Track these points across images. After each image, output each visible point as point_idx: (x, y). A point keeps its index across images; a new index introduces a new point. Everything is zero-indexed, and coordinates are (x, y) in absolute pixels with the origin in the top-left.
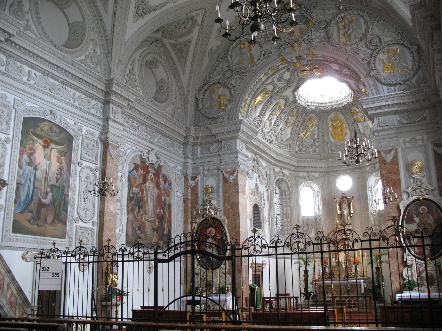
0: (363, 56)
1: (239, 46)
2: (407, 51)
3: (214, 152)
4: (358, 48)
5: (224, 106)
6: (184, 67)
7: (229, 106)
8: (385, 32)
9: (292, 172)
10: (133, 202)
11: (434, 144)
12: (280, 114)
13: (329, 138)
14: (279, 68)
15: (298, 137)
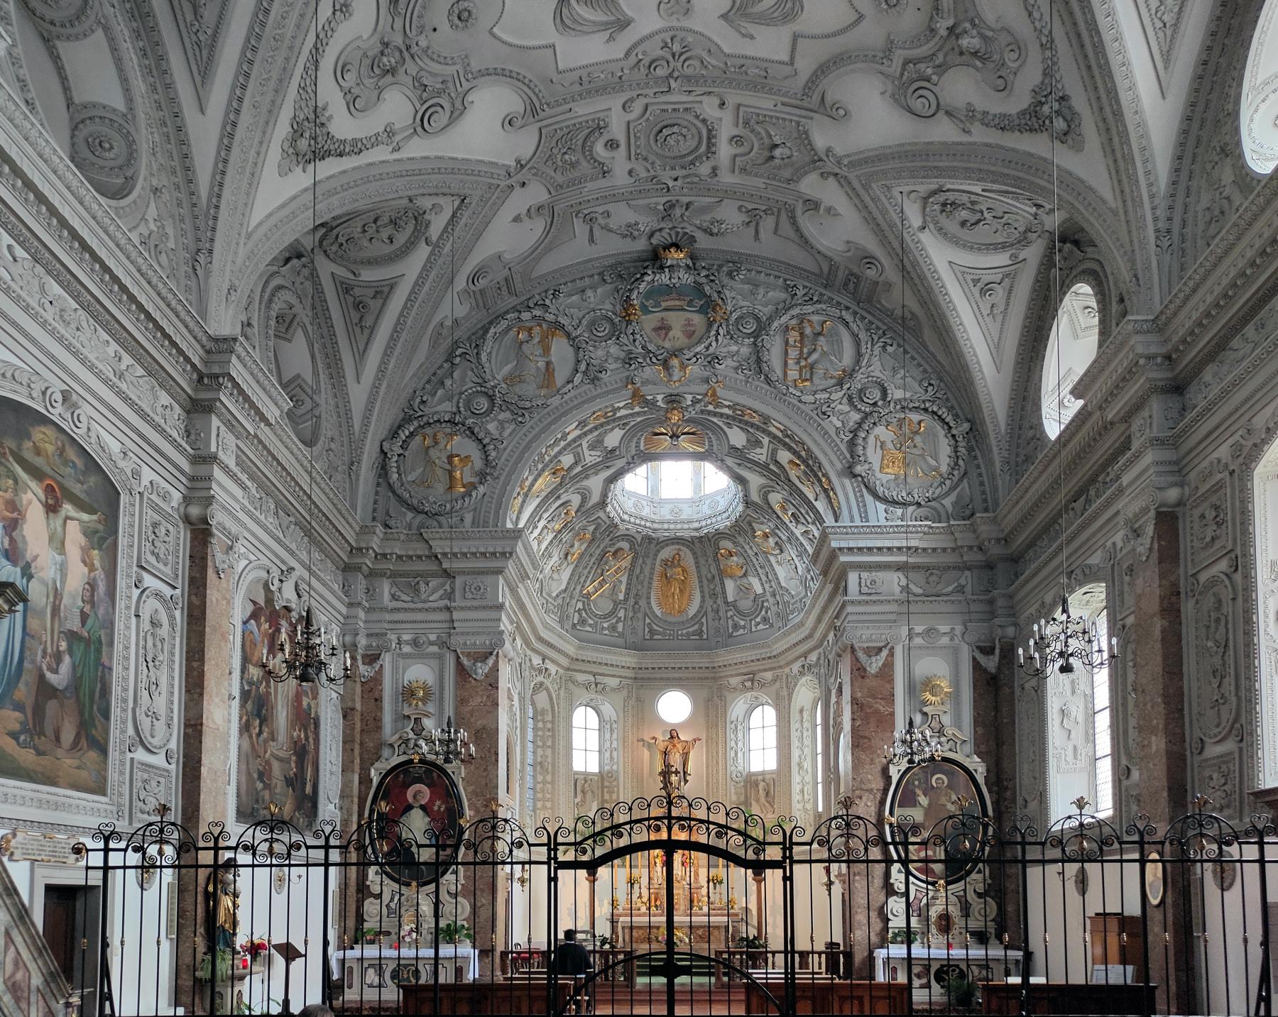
13: (649, 603)
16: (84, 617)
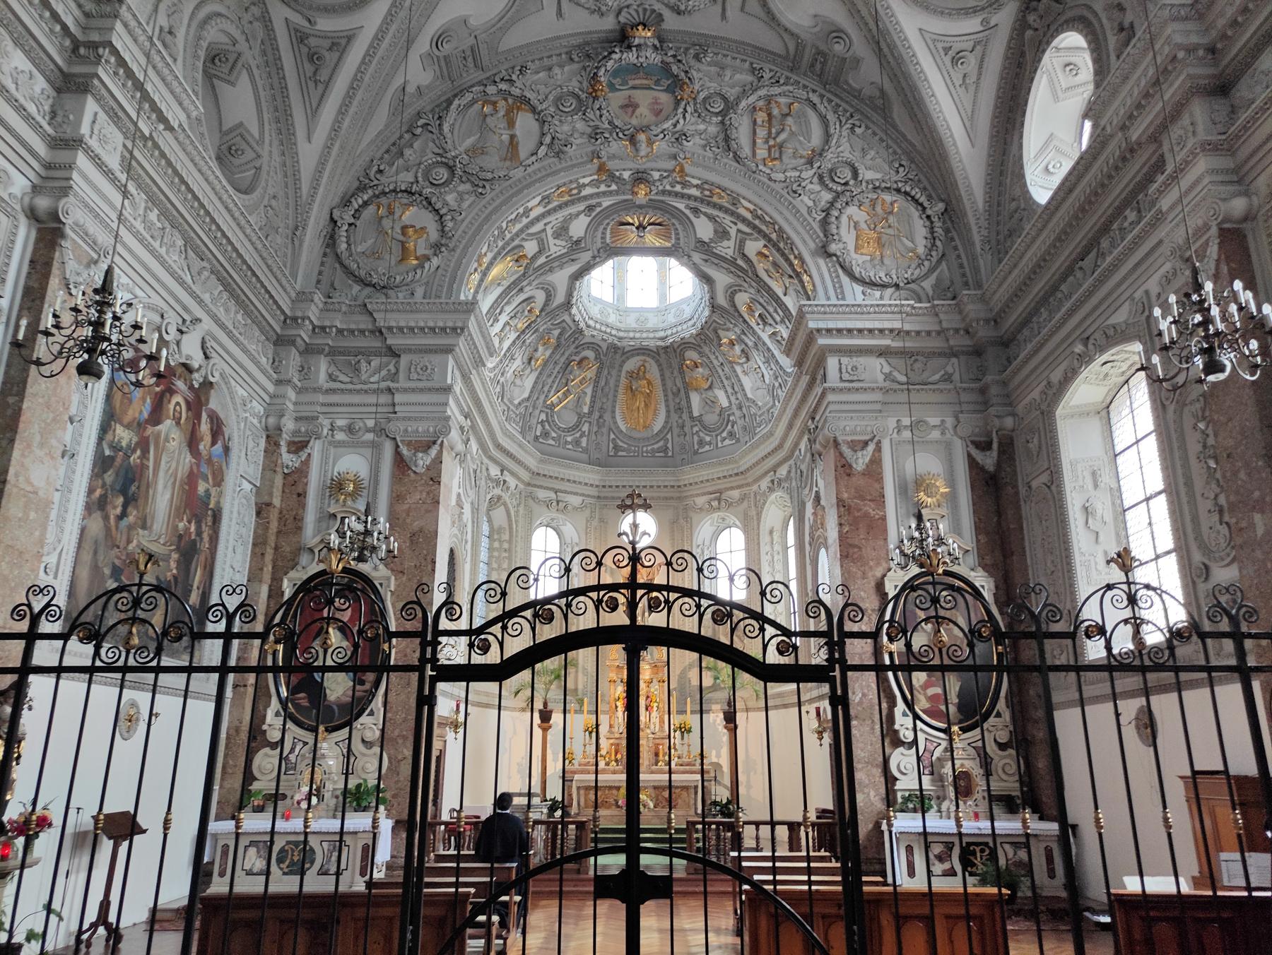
0: (810, 204)
1: (478, 106)
2: (914, 212)
3: (372, 380)
4: (799, 180)
5: (417, 259)
6: (313, 113)
7: (435, 261)
8: (869, 157)
9: (521, 486)
10: (109, 477)
11: (973, 442)
12: (523, 332)
13: (614, 417)
14: (580, 192)
15: (545, 402)
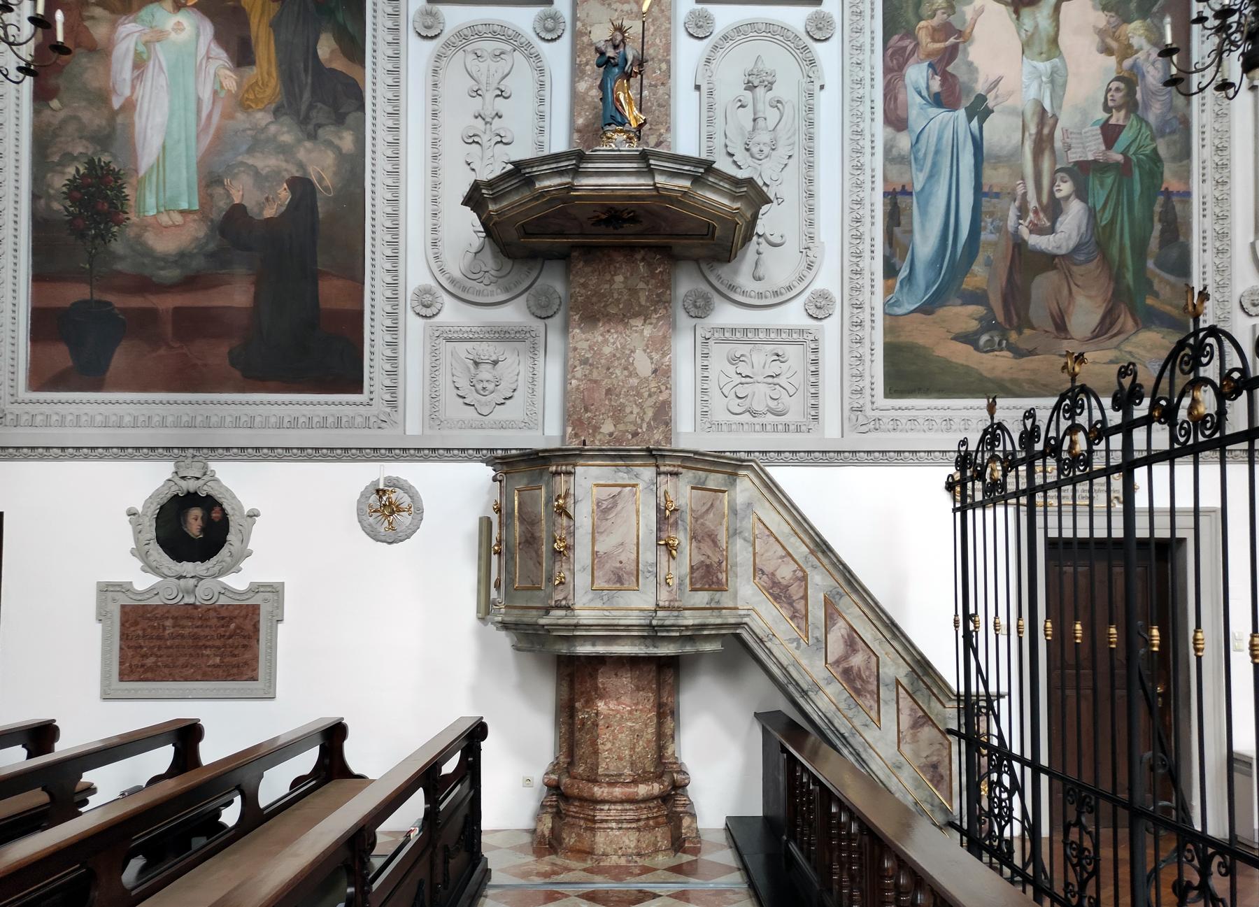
16: (1110, 134)
